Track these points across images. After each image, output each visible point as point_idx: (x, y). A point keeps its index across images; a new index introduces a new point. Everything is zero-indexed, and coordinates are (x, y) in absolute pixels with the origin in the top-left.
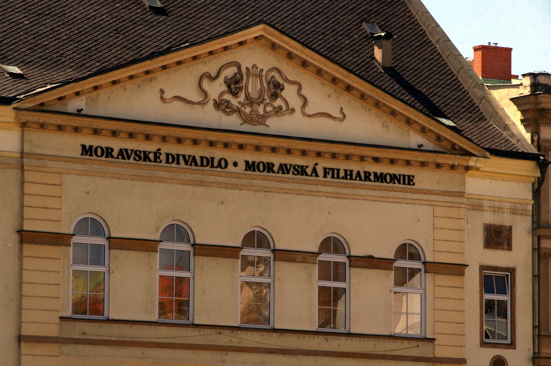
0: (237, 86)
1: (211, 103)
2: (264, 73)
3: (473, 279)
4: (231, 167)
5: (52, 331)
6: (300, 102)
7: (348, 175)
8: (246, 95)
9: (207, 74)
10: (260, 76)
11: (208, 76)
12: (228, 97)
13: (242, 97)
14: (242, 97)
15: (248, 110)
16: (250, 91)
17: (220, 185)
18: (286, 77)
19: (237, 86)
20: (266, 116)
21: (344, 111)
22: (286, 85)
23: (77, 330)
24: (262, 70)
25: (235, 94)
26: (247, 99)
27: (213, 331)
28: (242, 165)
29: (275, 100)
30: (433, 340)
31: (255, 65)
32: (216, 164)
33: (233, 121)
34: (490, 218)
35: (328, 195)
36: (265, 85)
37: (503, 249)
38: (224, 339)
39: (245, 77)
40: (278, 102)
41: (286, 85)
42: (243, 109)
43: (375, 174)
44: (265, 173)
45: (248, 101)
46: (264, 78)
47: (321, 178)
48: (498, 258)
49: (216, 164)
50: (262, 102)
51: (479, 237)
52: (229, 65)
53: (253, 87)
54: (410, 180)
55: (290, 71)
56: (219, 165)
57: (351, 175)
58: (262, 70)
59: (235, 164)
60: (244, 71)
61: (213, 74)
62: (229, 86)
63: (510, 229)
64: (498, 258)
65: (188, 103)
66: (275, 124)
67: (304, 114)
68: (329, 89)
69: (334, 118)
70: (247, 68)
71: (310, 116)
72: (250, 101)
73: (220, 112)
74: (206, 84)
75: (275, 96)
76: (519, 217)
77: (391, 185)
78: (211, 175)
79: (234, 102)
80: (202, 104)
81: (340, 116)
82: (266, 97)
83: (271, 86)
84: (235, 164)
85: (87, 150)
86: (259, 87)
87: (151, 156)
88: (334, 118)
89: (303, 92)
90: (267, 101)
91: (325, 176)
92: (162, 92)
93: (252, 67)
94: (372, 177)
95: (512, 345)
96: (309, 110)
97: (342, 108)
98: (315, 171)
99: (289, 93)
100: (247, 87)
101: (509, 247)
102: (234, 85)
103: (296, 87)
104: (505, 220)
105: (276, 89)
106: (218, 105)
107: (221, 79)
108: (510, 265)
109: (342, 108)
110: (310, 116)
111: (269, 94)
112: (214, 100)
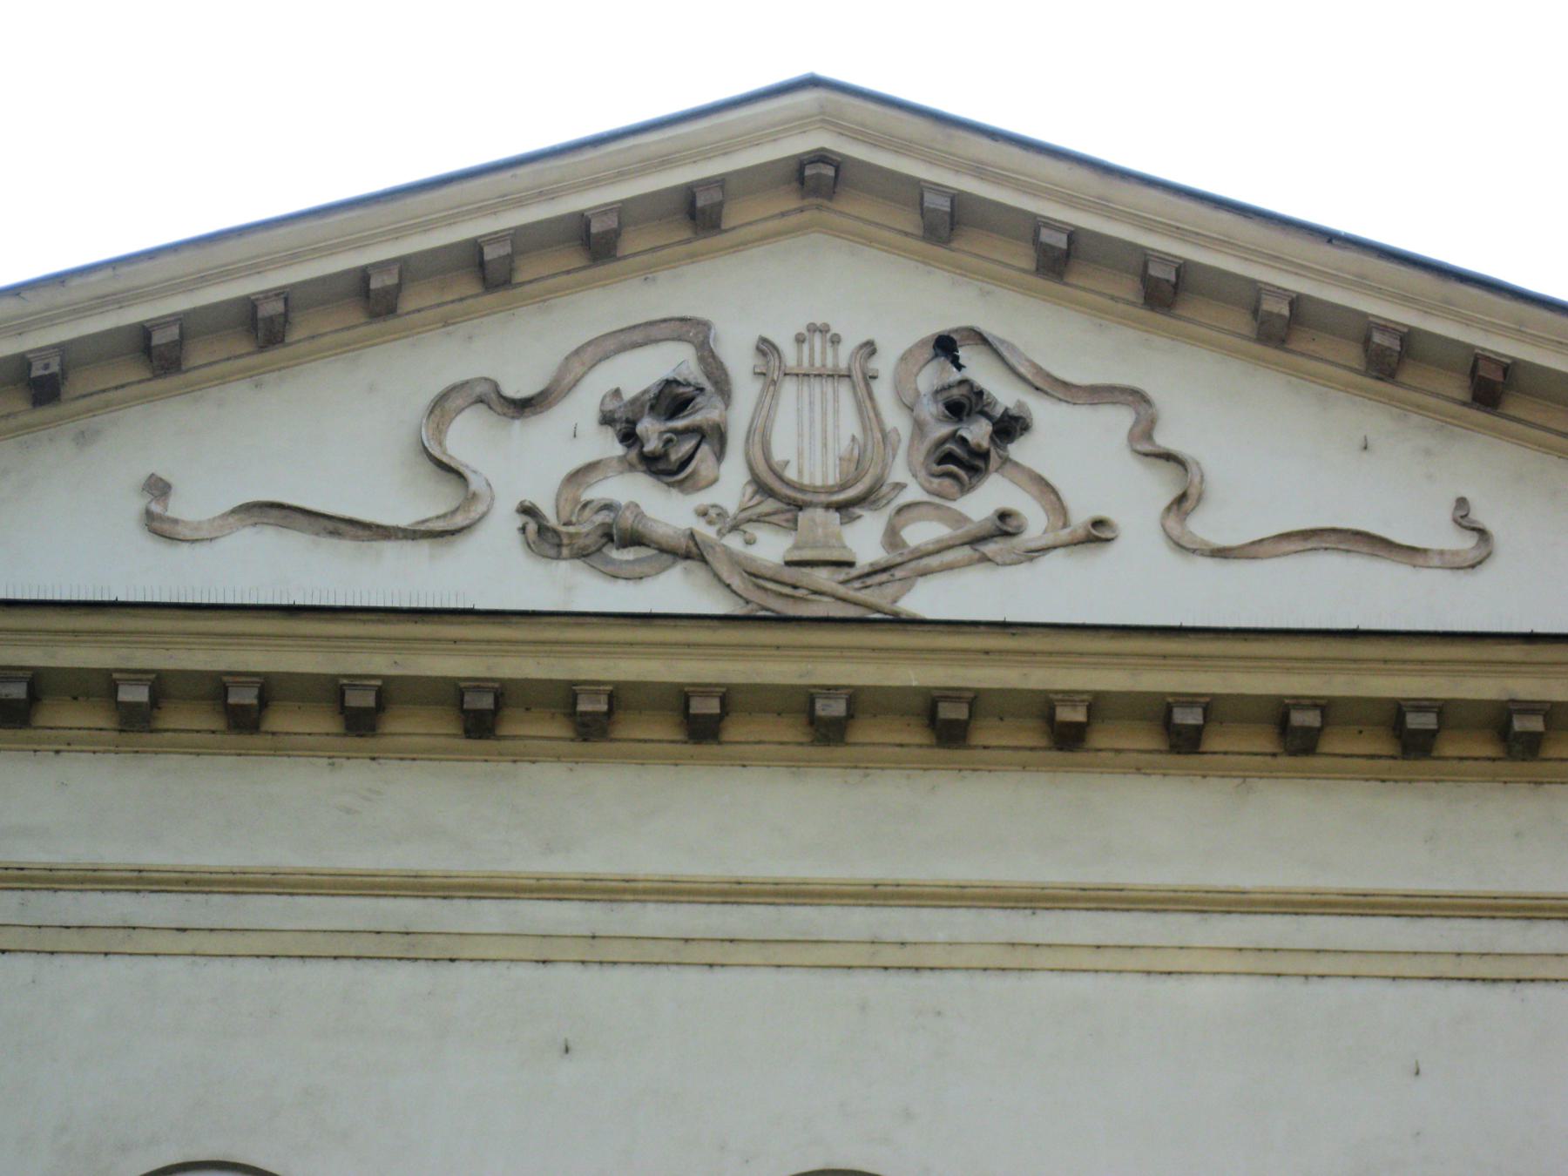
0: (679, 423)
1: (502, 528)
2: (884, 365)
6: (1158, 487)
8: (751, 469)
9: (480, 389)
10: (858, 376)
11: (481, 400)
14: (729, 486)
15: (771, 548)
16: (783, 448)
18: (1039, 370)
19: (679, 423)
20: (902, 565)
21: (1480, 516)
22: (1041, 410)
24: (870, 348)
25: (662, 467)
26: (762, 488)
29: (965, 489)
31: (823, 330)
36: (896, 420)
39: (746, 390)
41: (1041, 410)
42: (734, 542)
45: (770, 505)
46: (883, 391)
50: (867, 499)
52: (637, 336)
58: (870, 348)
60: (738, 359)
62: (629, 437)
65: (334, 533)
67: (1182, 547)
69: (1410, 554)
70: (765, 348)
71: (1221, 553)
72: (778, 497)
73: (564, 565)
74: (468, 439)
75: (962, 464)
79: (668, 511)
81: (1465, 543)
82: (899, 472)
83: (930, 410)
86: (849, 424)
88: (1410, 554)
89: (1165, 439)
90: (914, 493)
92: (158, 488)
93: (800, 340)
97: (1462, 502)
99: (1073, 452)
100: (760, 435)
102: (668, 430)
103: (1120, 419)
105: (972, 437)
106: (543, 536)
109: (1462, 502)
110: (1221, 553)
111: (920, 457)
112: (528, 511)
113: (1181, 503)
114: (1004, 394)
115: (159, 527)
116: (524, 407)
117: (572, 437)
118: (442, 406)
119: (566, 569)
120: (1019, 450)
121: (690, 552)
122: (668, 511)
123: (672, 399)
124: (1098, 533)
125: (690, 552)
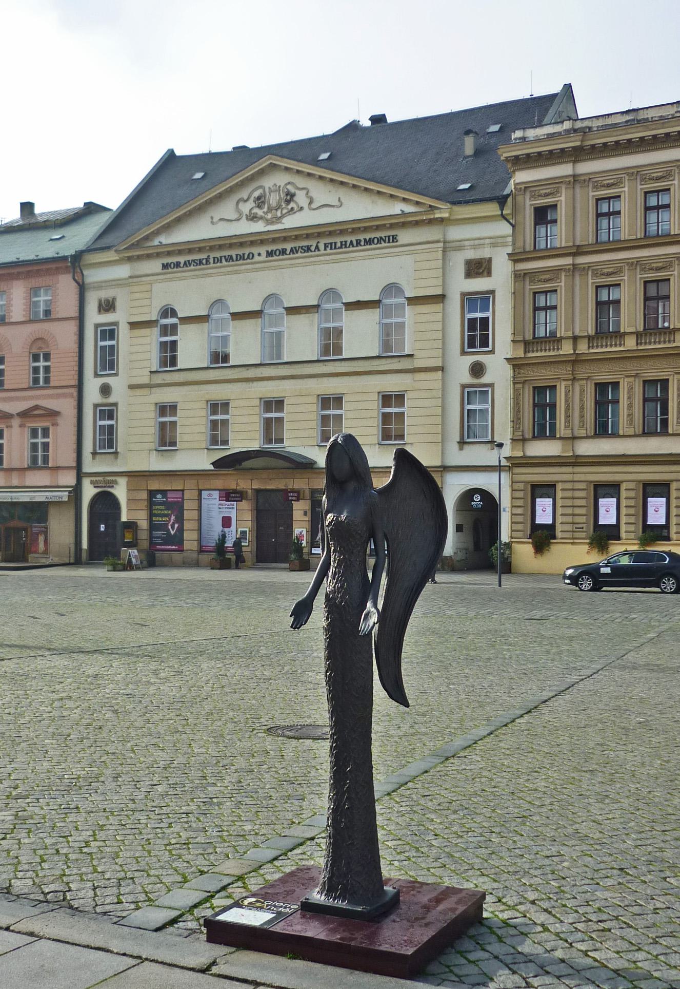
3: (454, 304)
4: (257, 258)
5: (145, 380)
7: (344, 245)
12: (256, 210)
13: (265, 210)
15: (269, 216)
17: (248, 271)
20: (283, 216)
22: (298, 192)
23: (158, 379)
25: (259, 207)
26: (268, 208)
27: (243, 369)
28: (264, 254)
30: (411, 356)
32: (246, 257)
33: (259, 227)
34: (471, 255)
35: (327, 262)
37: (483, 277)
38: (252, 373)
40: (289, 207)
41: (298, 192)
43: (365, 240)
44: (281, 257)
47: (322, 252)
48: (479, 284)
49: (246, 257)
51: (461, 269)
53: (273, 199)
54: (394, 238)
55: (300, 182)
56: (248, 257)
57: (346, 245)
59: (259, 255)
60: (267, 190)
61: (245, 198)
63: (490, 260)
64: (479, 284)
66: (290, 222)
68: (330, 187)
75: (288, 202)
76: (500, 248)
77: (379, 245)
78: (244, 266)
79: (260, 212)
80: (238, 220)
81: (338, 204)
84: (259, 255)
85: (165, 266)
87: (204, 261)
91: (325, 249)
92: (212, 218)
94: (362, 243)
95: (492, 352)
96: (313, 206)
98: (317, 248)
99: (301, 199)
101: (489, 274)
102: (260, 201)
103: (305, 192)
104: (485, 253)
105: (290, 197)
107: (252, 199)
108: (490, 288)
113: (310, 203)
114: (292, 190)
115: (213, 223)
116: (246, 201)
117: (251, 204)
118: (238, 203)
119: (251, 223)
120: (295, 198)
121: (261, 218)
122: (260, 212)
123: (259, 198)
124: (302, 208)
125: (261, 218)
